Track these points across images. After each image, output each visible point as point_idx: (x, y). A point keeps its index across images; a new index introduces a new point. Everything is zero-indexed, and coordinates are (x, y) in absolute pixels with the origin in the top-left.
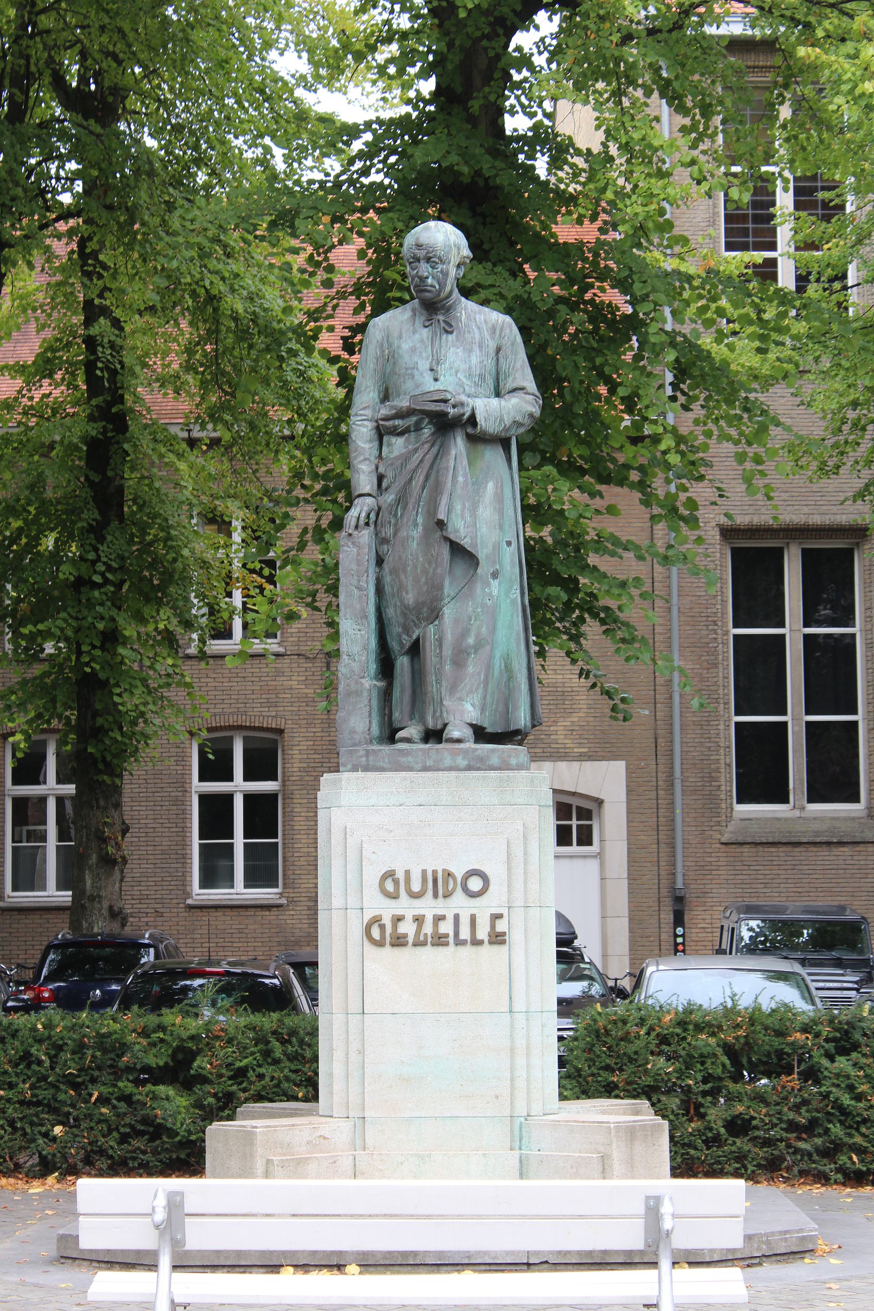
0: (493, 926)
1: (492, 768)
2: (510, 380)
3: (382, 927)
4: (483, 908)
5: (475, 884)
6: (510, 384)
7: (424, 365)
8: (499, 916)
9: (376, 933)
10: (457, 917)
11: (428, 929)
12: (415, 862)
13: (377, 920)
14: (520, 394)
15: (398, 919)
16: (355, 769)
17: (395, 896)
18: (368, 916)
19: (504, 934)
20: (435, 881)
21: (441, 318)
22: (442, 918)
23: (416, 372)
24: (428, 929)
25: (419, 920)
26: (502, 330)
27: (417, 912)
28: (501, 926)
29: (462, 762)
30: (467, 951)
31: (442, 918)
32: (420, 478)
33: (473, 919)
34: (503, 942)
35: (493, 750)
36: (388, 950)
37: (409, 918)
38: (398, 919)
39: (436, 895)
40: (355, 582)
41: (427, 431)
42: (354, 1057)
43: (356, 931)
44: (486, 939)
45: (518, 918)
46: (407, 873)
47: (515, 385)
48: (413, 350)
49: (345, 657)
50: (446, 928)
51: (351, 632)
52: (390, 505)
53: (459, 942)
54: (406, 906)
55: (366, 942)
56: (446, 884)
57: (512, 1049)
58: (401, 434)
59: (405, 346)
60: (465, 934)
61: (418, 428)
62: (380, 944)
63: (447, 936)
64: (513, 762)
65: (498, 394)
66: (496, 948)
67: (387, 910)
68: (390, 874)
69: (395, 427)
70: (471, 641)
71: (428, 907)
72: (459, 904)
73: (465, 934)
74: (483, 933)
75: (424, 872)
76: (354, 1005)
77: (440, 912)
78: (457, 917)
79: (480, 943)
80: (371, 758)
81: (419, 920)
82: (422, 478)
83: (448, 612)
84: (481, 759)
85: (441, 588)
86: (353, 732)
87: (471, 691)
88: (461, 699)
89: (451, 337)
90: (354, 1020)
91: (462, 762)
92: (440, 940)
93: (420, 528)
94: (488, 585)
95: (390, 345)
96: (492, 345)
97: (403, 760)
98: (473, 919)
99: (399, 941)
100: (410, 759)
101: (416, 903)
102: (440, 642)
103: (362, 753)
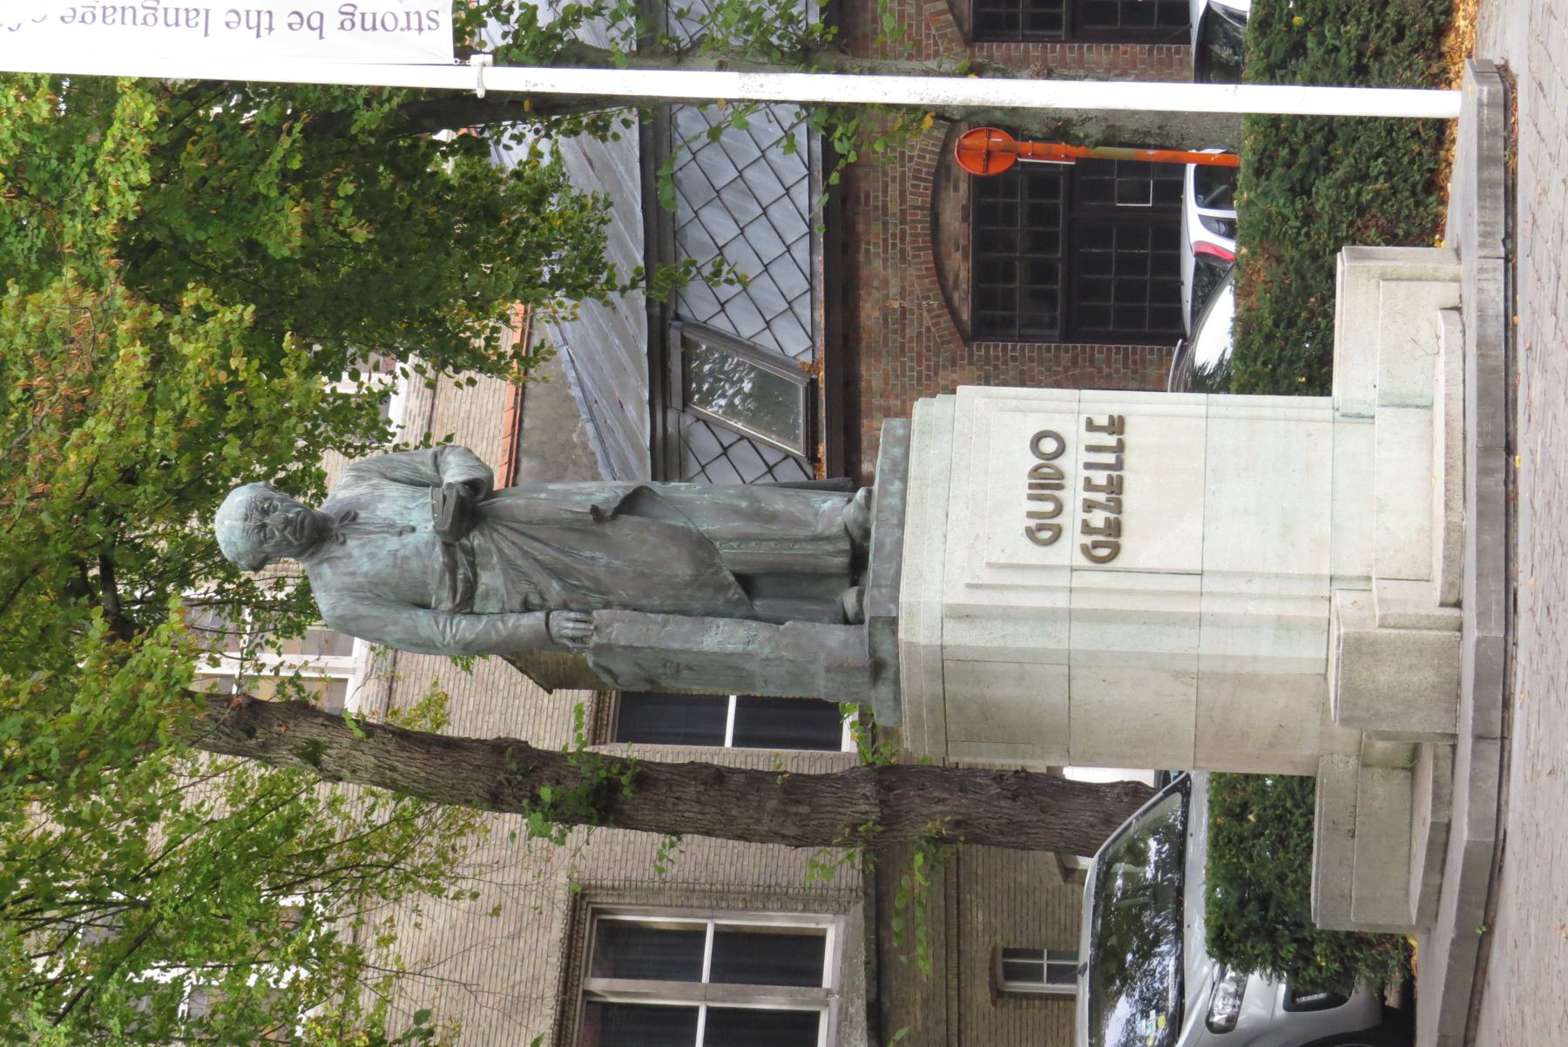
1: (906, 456)
2: (423, 468)
3: (1096, 545)
6: (428, 470)
7: (393, 543)
10: (1088, 466)
11: (1101, 497)
12: (1020, 506)
13: (1086, 550)
16: (895, 601)
18: (1082, 561)
19: (1111, 417)
20: (1042, 486)
22: (1088, 480)
23: (400, 554)
24: (1101, 497)
25: (1089, 506)
26: (359, 470)
27: (1079, 505)
28: (1104, 422)
29: (896, 486)
30: (1130, 457)
31: (1088, 480)
32: (534, 548)
33: (1091, 449)
34: (1121, 419)
35: (885, 452)
36: (1125, 541)
39: (1060, 487)
40: (657, 627)
41: (477, 540)
42: (1256, 587)
43: (1099, 578)
47: (430, 462)
48: (372, 556)
49: (750, 648)
50: (1100, 478)
51: (719, 638)
52: (564, 588)
53: (1119, 465)
54: (1072, 519)
55: (1117, 563)
57: (1251, 418)
58: (475, 575)
59: (365, 566)
60: (1110, 458)
61: (470, 553)
62: (1116, 550)
63: (1110, 478)
64: (900, 432)
66: (1128, 428)
67: (1073, 539)
68: (1031, 533)
69: (466, 580)
70: (744, 504)
71: (1073, 496)
73: (1110, 458)
74: (1111, 441)
75: (1031, 497)
76: (1192, 584)
77: (1081, 483)
78: (1088, 466)
80: (883, 582)
81: (1089, 506)
82: (535, 544)
83: (706, 526)
84: (893, 469)
85: (676, 529)
86: (845, 644)
87: (808, 504)
88: (816, 514)
89: (362, 514)
90: (1210, 585)
91: (896, 486)
93: (597, 554)
95: (361, 587)
97: (888, 547)
98: (1091, 449)
99: (1114, 528)
100: (888, 540)
101: (1067, 508)
102: (744, 539)
103: (876, 592)
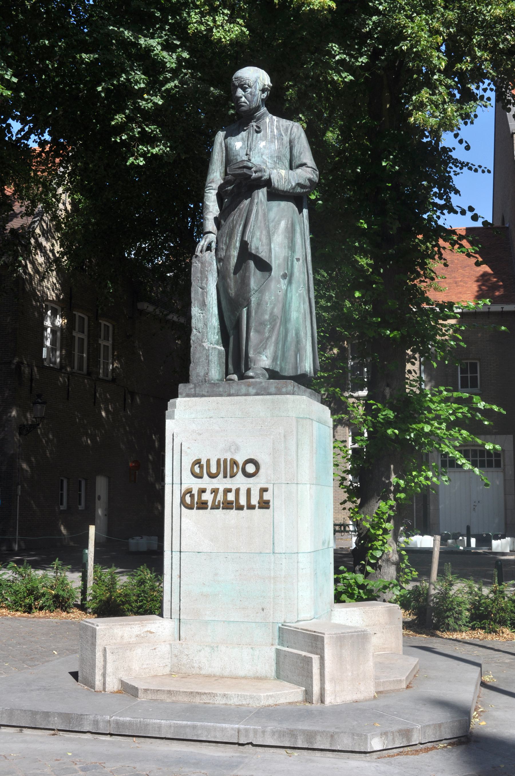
0: (261, 496)
3: (192, 496)
5: (250, 468)
6: (297, 162)
8: (265, 490)
9: (188, 499)
10: (238, 491)
13: (189, 491)
14: (304, 168)
15: (203, 491)
16: (188, 396)
17: (199, 476)
18: (184, 487)
21: (254, 124)
22: (230, 491)
24: (220, 497)
25: (215, 491)
28: (266, 496)
30: (246, 512)
31: (230, 491)
33: (249, 491)
34: (268, 508)
37: (208, 491)
38: (203, 491)
39: (225, 477)
42: (176, 579)
44: (257, 505)
46: (208, 461)
47: (299, 163)
50: (231, 497)
53: (240, 508)
54: (206, 483)
56: (232, 468)
62: (190, 507)
65: (291, 168)
67: (195, 485)
68: (198, 462)
72: (240, 482)
73: (243, 501)
74: (254, 501)
75: (218, 461)
77: (228, 486)
80: (197, 389)
81: (215, 491)
92: (228, 505)
94: (279, 282)
96: (286, 139)
98: (249, 491)
99: (203, 505)
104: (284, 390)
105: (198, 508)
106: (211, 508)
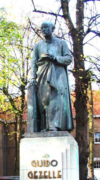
3: (32, 174)
4: (56, 169)
5: (54, 163)
9: (30, 175)
11: (43, 174)
12: (39, 158)
13: (30, 172)
14: (67, 56)
15: (35, 172)
22: (46, 172)
24: (43, 174)
25: (41, 172)
28: (61, 174)
31: (46, 172)
38: (35, 172)
45: (65, 171)
47: (66, 54)
50: (47, 174)
53: (50, 178)
54: (38, 169)
62: (31, 178)
63: (47, 176)
65: (62, 56)
67: (33, 170)
71: (43, 169)
74: (56, 175)
75: (42, 161)
79: (51, 178)
81: (41, 172)
94: (60, 96)
96: (61, 46)
104: (65, 135)
105: (34, 178)
106: (40, 178)
